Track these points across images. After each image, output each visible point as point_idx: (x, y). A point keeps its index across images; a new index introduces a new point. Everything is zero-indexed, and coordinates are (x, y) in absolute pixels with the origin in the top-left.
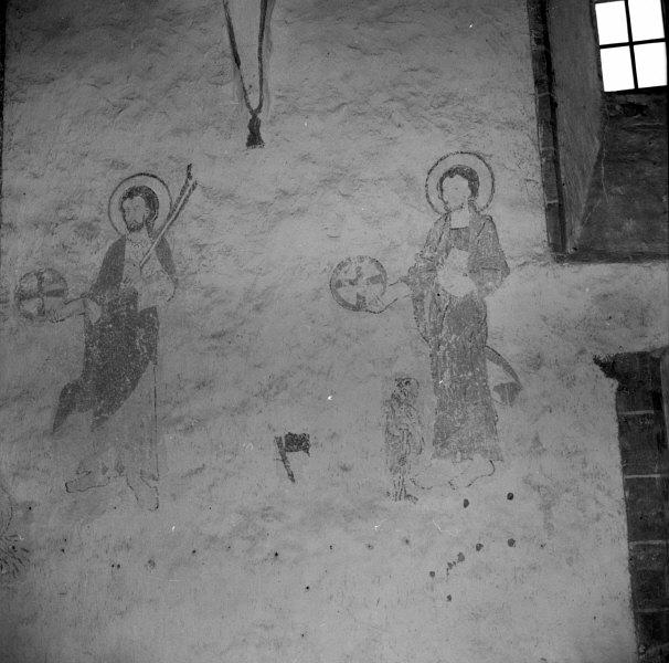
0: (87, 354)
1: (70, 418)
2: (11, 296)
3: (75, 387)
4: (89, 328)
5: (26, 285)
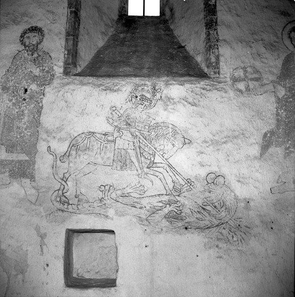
0: (278, 114)
1: (272, 150)
2: (228, 79)
3: (272, 133)
4: (279, 100)
5: (236, 74)
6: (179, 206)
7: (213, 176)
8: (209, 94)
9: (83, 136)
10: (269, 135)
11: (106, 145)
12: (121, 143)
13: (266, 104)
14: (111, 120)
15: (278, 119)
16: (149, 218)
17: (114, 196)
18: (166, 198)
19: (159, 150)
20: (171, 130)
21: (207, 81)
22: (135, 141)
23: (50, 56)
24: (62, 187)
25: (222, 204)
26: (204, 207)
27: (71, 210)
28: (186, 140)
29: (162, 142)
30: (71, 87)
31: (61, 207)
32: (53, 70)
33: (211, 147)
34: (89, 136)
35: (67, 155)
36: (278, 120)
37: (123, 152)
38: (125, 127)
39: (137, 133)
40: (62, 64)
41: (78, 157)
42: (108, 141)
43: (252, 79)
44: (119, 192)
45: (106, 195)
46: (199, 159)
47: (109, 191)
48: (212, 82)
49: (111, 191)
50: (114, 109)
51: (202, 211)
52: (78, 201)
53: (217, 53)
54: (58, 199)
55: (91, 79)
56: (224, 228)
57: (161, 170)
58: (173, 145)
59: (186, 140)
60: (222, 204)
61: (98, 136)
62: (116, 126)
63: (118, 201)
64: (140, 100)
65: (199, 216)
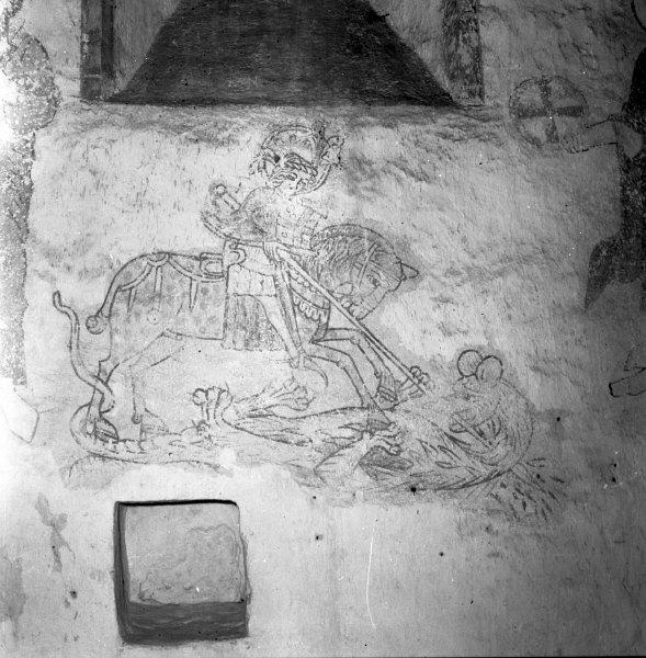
0: (625, 200)
1: (611, 289)
2: (506, 111)
3: (612, 246)
4: (627, 165)
5: (523, 97)
6: (394, 436)
7: (473, 357)
8: (458, 150)
9: (144, 263)
10: (604, 253)
11: (204, 285)
12: (243, 280)
13: (594, 171)
14: (211, 220)
15: (626, 212)
16: (322, 468)
17: (230, 415)
18: (360, 417)
19: (339, 296)
20: (367, 244)
21: (453, 117)
22: (279, 273)
23: (44, 50)
24: (98, 397)
25: (497, 427)
26: (454, 435)
27: (123, 454)
28: (405, 268)
29: (347, 274)
30: (105, 133)
31: (98, 446)
32: (54, 87)
33: (467, 286)
34: (160, 263)
35: (104, 313)
36: (625, 214)
37: (249, 303)
38: (252, 237)
39: (284, 255)
40: (75, 70)
41: (133, 319)
42: (209, 275)
43: (562, 112)
44: (244, 407)
45: (211, 416)
46: (437, 316)
47: (217, 404)
48: (466, 119)
49: (224, 404)
50: (220, 190)
51: (451, 446)
52: (142, 431)
53: (476, 44)
54: (90, 429)
55: (156, 112)
56: (503, 486)
57: (346, 346)
58: (375, 282)
59: (405, 268)
60: (497, 427)
61: (180, 258)
62: (228, 237)
63: (242, 429)
64: (287, 166)
65: (442, 457)
